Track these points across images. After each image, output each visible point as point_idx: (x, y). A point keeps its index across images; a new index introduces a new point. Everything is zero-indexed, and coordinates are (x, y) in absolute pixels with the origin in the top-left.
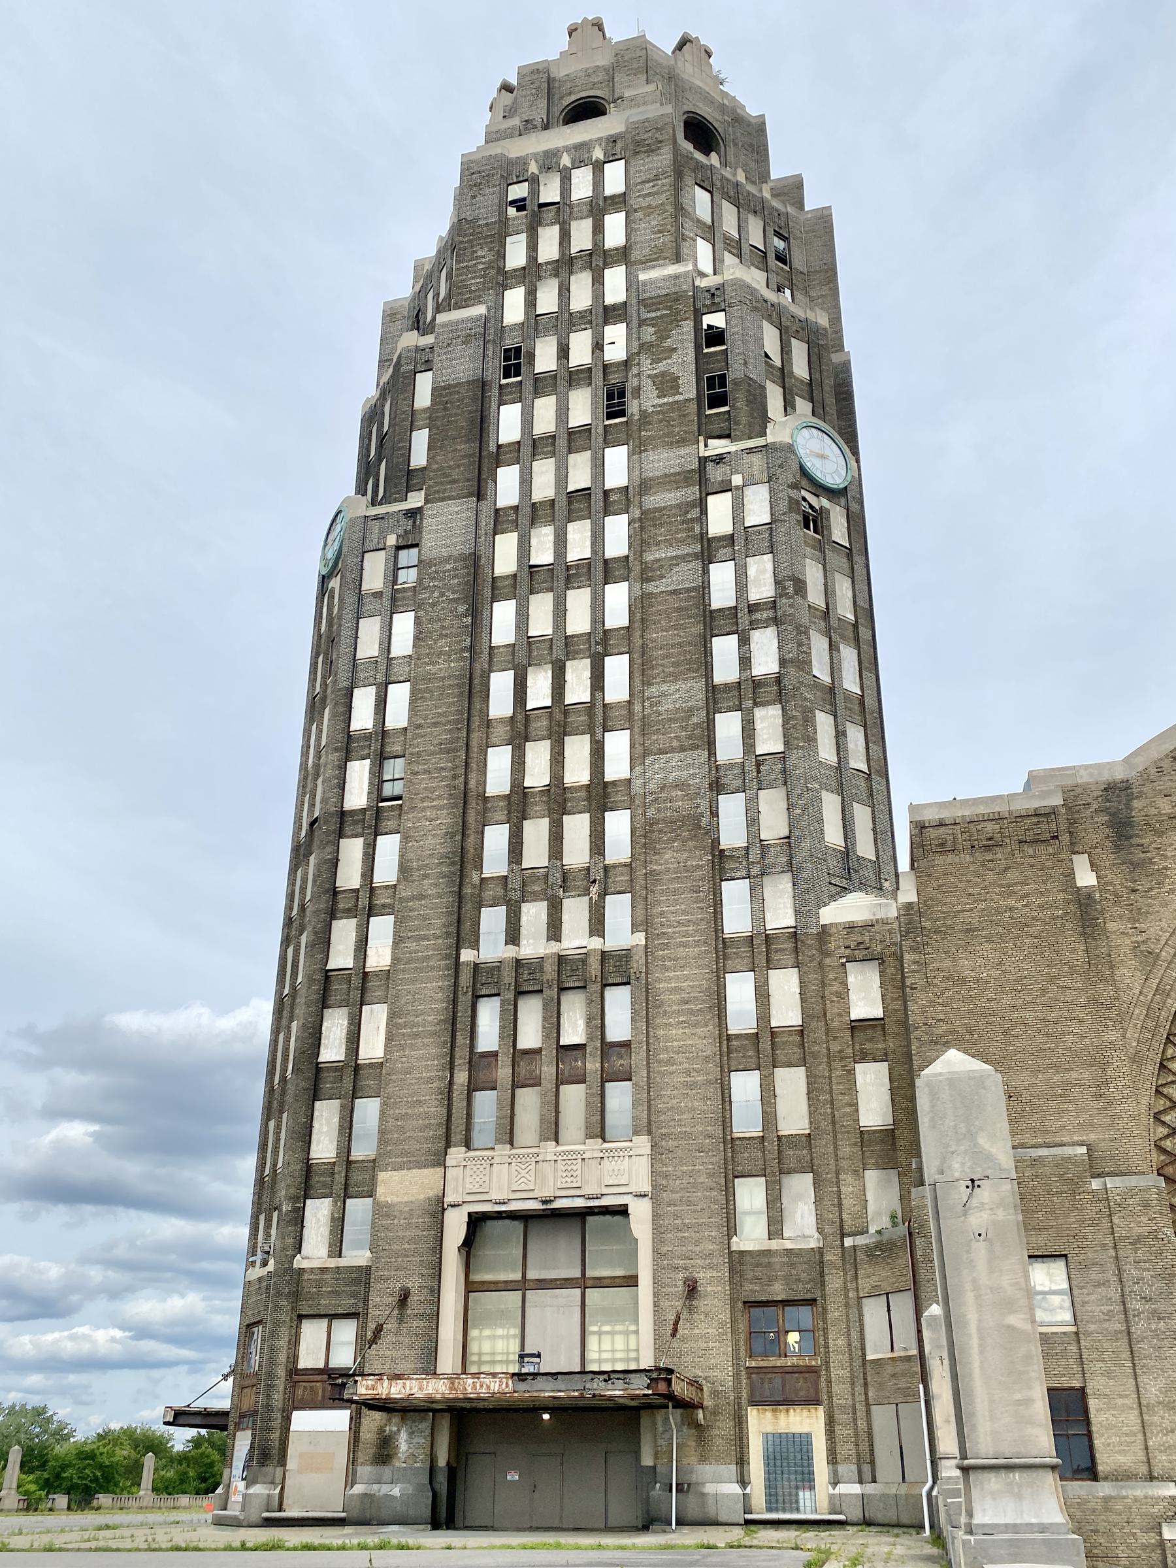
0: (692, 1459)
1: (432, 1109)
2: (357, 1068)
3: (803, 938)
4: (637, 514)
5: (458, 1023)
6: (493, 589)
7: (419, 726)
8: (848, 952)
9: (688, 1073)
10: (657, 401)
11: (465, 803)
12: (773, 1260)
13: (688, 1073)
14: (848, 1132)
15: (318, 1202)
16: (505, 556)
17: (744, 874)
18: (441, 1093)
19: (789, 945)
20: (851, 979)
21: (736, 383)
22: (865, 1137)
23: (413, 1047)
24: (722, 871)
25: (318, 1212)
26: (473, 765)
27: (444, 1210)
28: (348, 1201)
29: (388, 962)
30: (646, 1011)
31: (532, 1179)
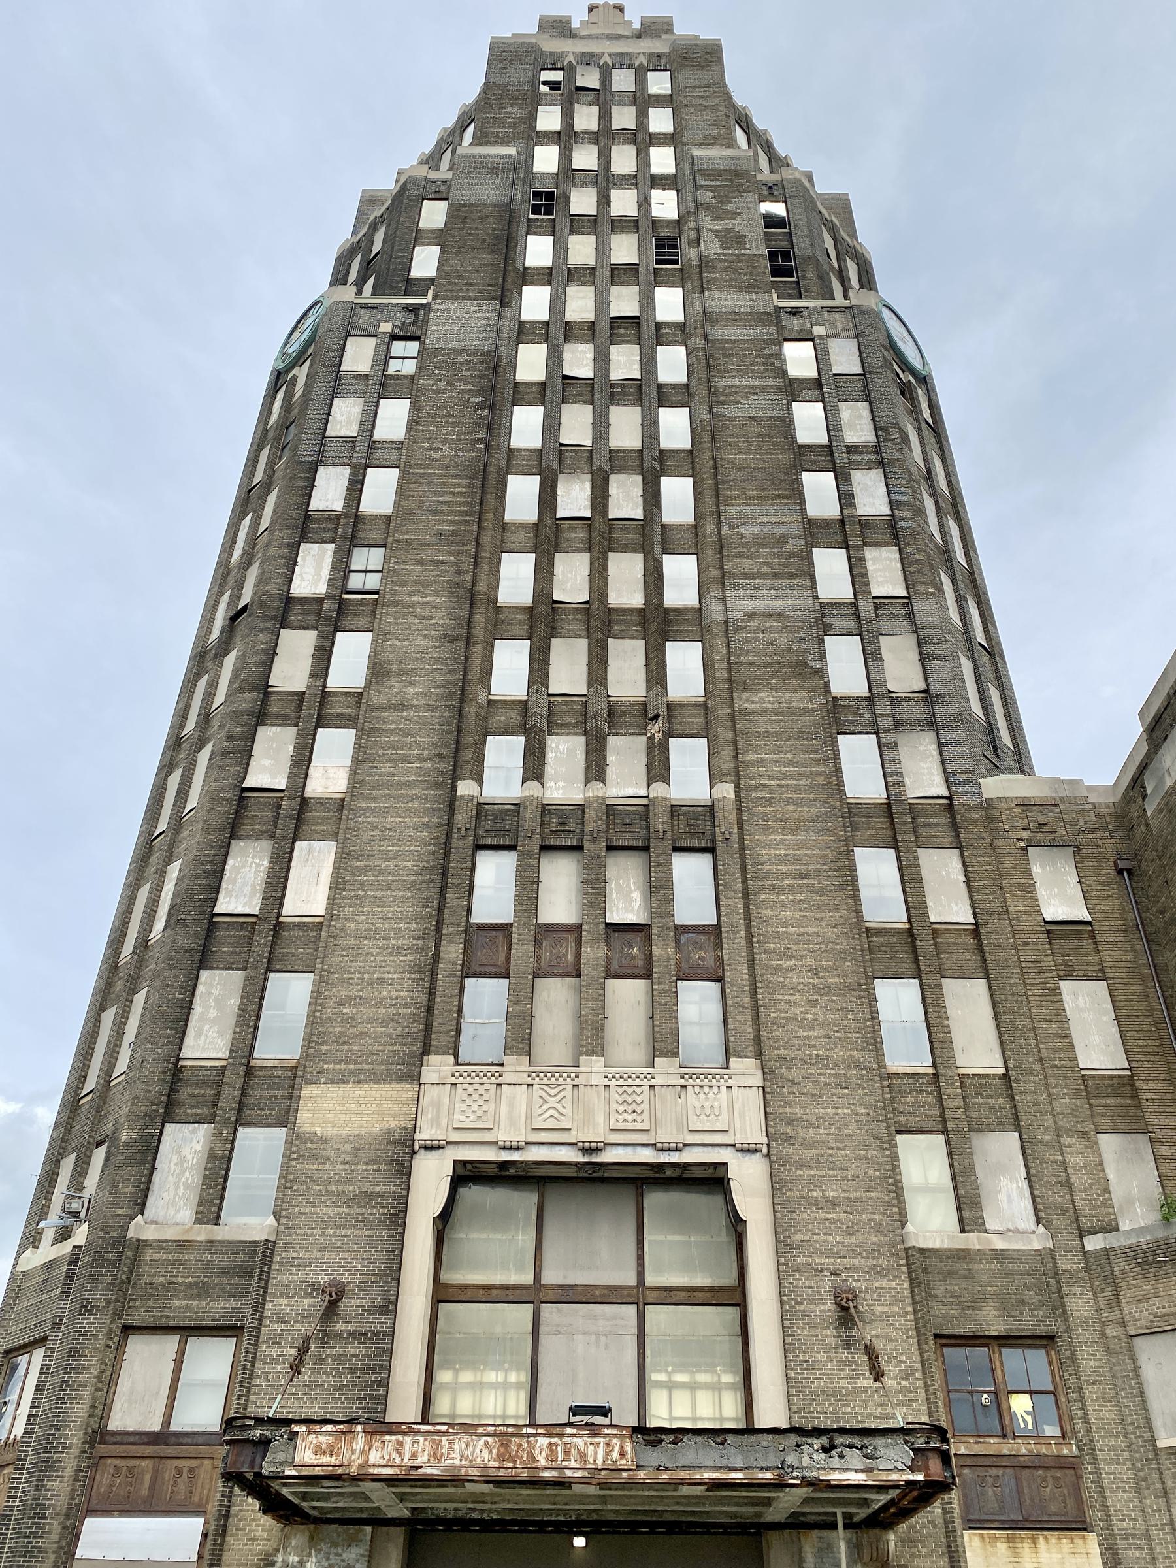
2: (278, 927)
4: (701, 344)
5: (447, 880)
6: (514, 393)
7: (411, 512)
10: (720, 251)
11: (472, 605)
15: (186, 1128)
16: (531, 363)
18: (420, 971)
21: (805, 260)
23: (376, 901)
25: (184, 1146)
26: (484, 565)
27: (414, 1152)
28: (241, 1130)
29: (343, 788)
31: (568, 1111)
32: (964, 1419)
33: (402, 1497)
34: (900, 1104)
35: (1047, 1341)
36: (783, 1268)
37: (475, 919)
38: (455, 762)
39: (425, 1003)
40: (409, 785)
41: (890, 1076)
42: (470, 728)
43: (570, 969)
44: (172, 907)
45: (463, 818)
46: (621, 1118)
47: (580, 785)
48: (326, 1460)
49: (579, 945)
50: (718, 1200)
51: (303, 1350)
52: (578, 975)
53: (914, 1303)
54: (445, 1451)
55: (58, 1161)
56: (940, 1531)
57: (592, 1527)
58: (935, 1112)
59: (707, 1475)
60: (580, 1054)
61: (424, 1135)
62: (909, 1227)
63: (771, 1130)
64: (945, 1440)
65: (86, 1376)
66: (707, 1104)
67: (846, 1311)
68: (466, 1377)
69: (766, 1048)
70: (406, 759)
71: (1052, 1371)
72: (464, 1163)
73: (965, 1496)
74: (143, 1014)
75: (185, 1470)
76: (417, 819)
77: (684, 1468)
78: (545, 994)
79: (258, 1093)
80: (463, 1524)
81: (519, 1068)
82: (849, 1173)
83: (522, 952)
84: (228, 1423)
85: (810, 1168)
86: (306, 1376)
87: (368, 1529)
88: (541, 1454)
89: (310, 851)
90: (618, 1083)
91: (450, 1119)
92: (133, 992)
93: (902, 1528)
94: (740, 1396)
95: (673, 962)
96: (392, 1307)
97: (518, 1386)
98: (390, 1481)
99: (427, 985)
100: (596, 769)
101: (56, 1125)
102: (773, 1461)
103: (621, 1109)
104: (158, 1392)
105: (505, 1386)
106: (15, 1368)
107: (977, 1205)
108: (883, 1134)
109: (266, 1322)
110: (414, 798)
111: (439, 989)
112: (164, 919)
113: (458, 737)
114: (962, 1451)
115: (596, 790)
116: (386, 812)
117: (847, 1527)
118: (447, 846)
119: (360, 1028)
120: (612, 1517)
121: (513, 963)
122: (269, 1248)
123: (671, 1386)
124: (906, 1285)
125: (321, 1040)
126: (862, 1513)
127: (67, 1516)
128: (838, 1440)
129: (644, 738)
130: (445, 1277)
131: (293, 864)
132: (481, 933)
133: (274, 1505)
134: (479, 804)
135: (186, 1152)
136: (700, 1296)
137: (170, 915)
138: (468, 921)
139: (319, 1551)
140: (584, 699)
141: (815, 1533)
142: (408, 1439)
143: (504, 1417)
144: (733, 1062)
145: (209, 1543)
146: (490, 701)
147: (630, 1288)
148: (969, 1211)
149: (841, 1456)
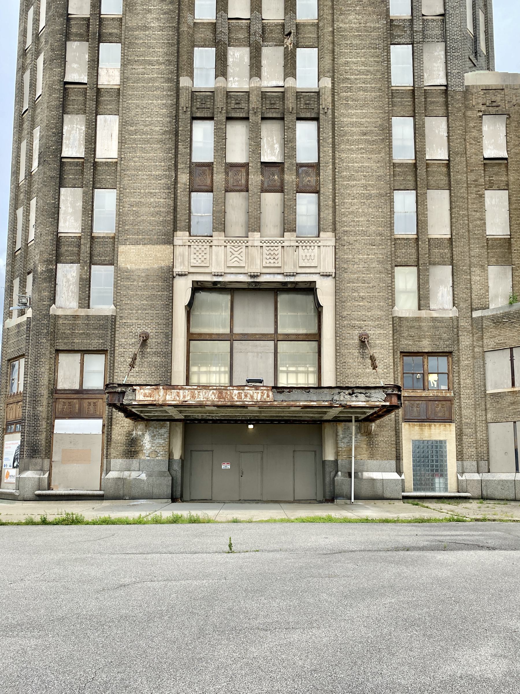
0: (364, 456)
1: (160, 200)
2: (95, 164)
3: (452, 94)
8: (483, 108)
9: (365, 187)
12: (423, 324)
13: (365, 187)
14: (478, 239)
17: (408, 40)
18: (168, 188)
19: (442, 100)
20: (485, 128)
22: (491, 244)
24: (392, 36)
25: (68, 274)
27: (174, 277)
28: (93, 266)
30: (331, 139)
31: (243, 259)
32: (408, 382)
33: (181, 412)
34: (398, 253)
35: (448, 354)
36: (338, 326)
37: (195, 160)
38: (178, 65)
39: (173, 205)
40: (153, 80)
41: (395, 239)
42: (185, 42)
43: (243, 188)
44: (40, 154)
45: (184, 101)
46: (268, 261)
47: (247, 79)
48: (149, 399)
49: (248, 174)
50: (311, 298)
51: (134, 359)
52: (247, 191)
53: (394, 339)
54: (197, 395)
55: (12, 281)
56: (393, 423)
57: (256, 421)
58: (414, 257)
59: (301, 403)
60: (249, 231)
61: (177, 269)
62: (396, 308)
63: (337, 266)
64: (400, 391)
65: (44, 369)
66: (308, 255)
67: (363, 343)
68: (203, 369)
69: (338, 227)
70: (150, 63)
71: (448, 365)
72: (197, 282)
73: (405, 411)
74: (36, 211)
75: (92, 403)
76: (159, 101)
77: (293, 401)
78: (231, 201)
79: (98, 249)
80: (206, 421)
81: (220, 238)
82: (371, 285)
83: (219, 178)
84: (107, 386)
85: (354, 283)
86: (136, 369)
87: (168, 423)
88: (235, 396)
89: (105, 121)
90: (267, 245)
91: (189, 262)
92: (29, 199)
93: (378, 422)
94: (316, 376)
95: (294, 183)
96: (170, 342)
97: (225, 372)
98: (175, 406)
99: (173, 196)
100: (256, 68)
101: (7, 265)
102: (329, 398)
103: (268, 257)
104: (75, 375)
105: (220, 372)
106: (14, 366)
107: (427, 298)
108: (389, 267)
109: (117, 348)
110: (157, 88)
111: (179, 198)
112: (37, 160)
113: (178, 48)
114: (406, 395)
115: (255, 83)
116: (143, 97)
117: (356, 421)
118: (177, 116)
119: (142, 218)
120: (264, 418)
121: (215, 184)
122: (113, 320)
123: (288, 372)
124: (391, 332)
125: (124, 223)
126: (363, 416)
127: (48, 419)
128: (356, 391)
129: (282, 48)
130: (192, 330)
131: (98, 128)
132: (197, 167)
133: (129, 414)
134: (193, 92)
135: (69, 276)
136: (301, 338)
137: (40, 158)
138: (190, 161)
139: (149, 430)
140: (248, 21)
141: (343, 424)
142: (181, 392)
143: (219, 383)
144: (322, 234)
145: (106, 428)
146: (195, 23)
147: (272, 334)
148: (423, 299)
149: (356, 396)
